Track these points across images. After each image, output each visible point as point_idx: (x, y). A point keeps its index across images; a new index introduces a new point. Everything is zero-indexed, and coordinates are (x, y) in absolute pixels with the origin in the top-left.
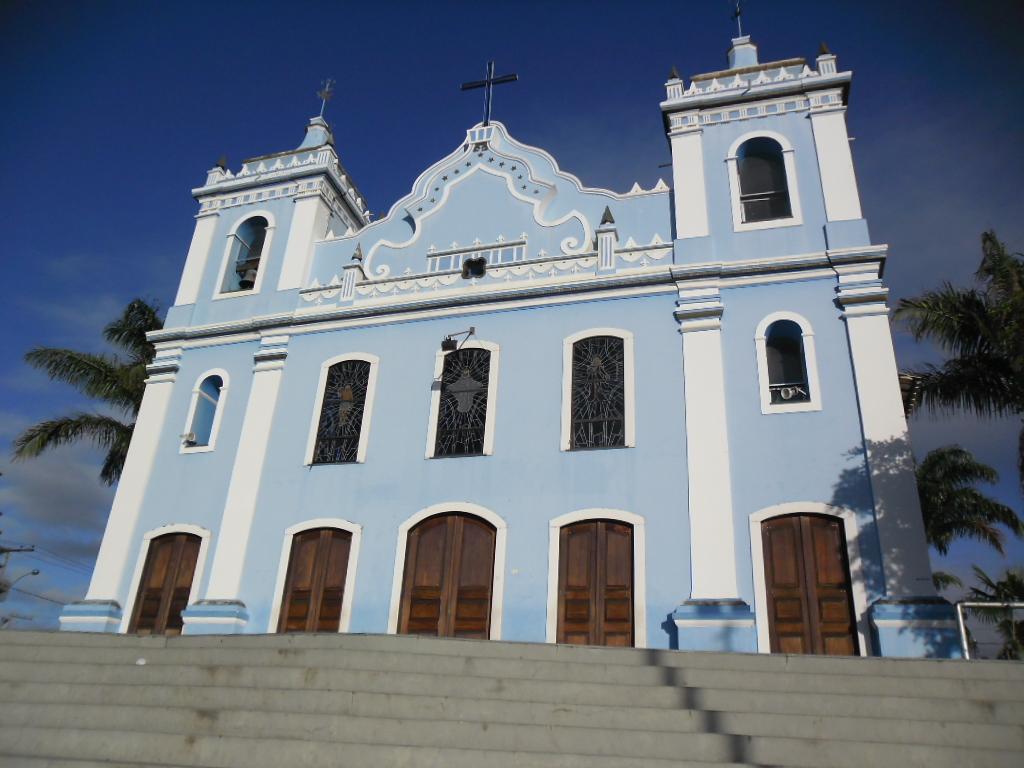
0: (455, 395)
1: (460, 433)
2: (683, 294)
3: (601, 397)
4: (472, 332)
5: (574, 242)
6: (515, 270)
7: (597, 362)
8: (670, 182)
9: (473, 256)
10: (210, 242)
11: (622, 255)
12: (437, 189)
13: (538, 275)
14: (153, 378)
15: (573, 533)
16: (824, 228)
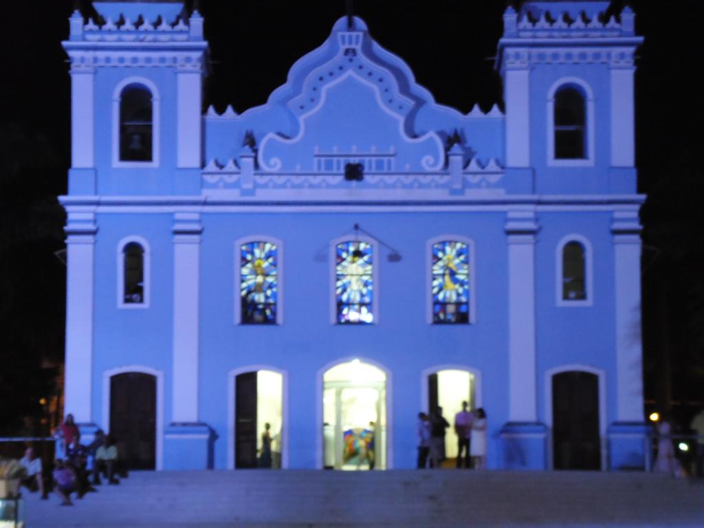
2: (511, 215)
4: (356, 227)
5: (432, 160)
6: (386, 178)
8: (502, 108)
12: (315, 89)
13: (404, 186)
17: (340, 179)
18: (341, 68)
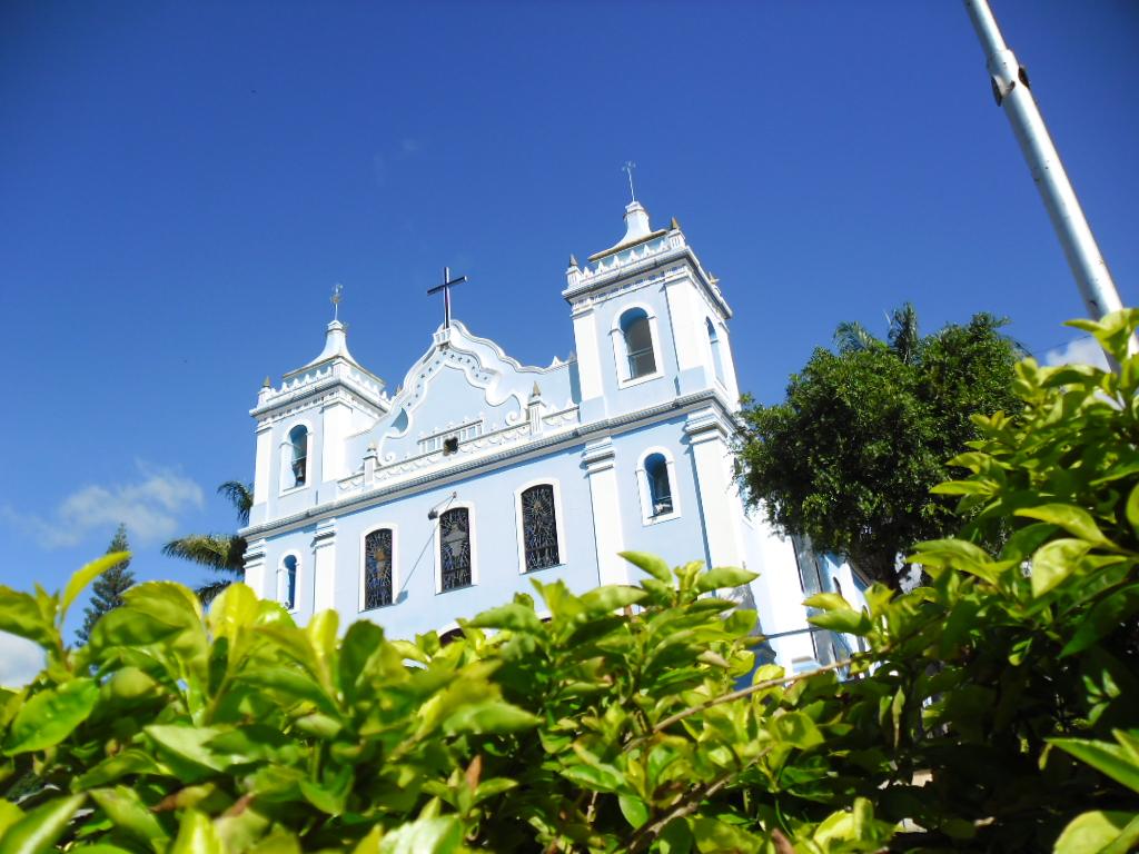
0: (451, 545)
1: (456, 573)
3: (542, 530)
5: (515, 415)
6: (477, 443)
7: (538, 504)
9: (450, 437)
10: (271, 452)
11: (549, 421)
14: (248, 564)
16: (676, 381)
17: (441, 453)
18: (438, 363)
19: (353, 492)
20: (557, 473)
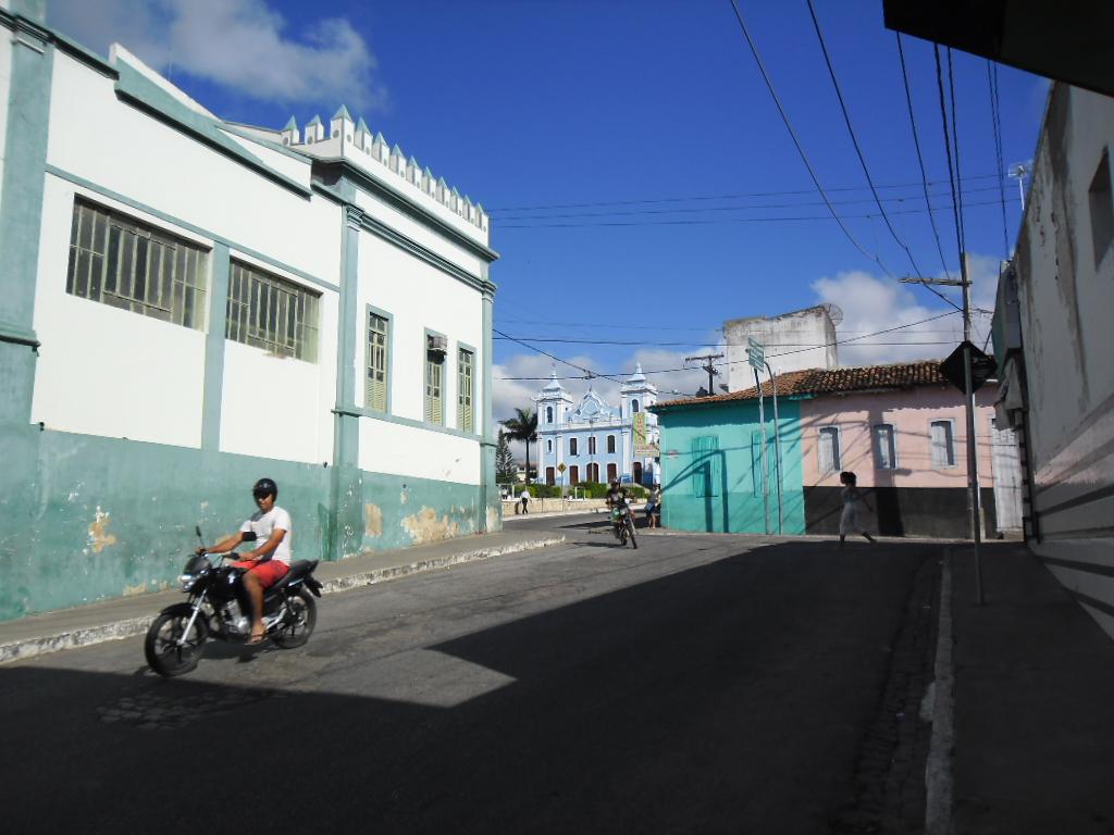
1: (592, 450)
15: (609, 465)
19: (567, 428)
20: (615, 433)
